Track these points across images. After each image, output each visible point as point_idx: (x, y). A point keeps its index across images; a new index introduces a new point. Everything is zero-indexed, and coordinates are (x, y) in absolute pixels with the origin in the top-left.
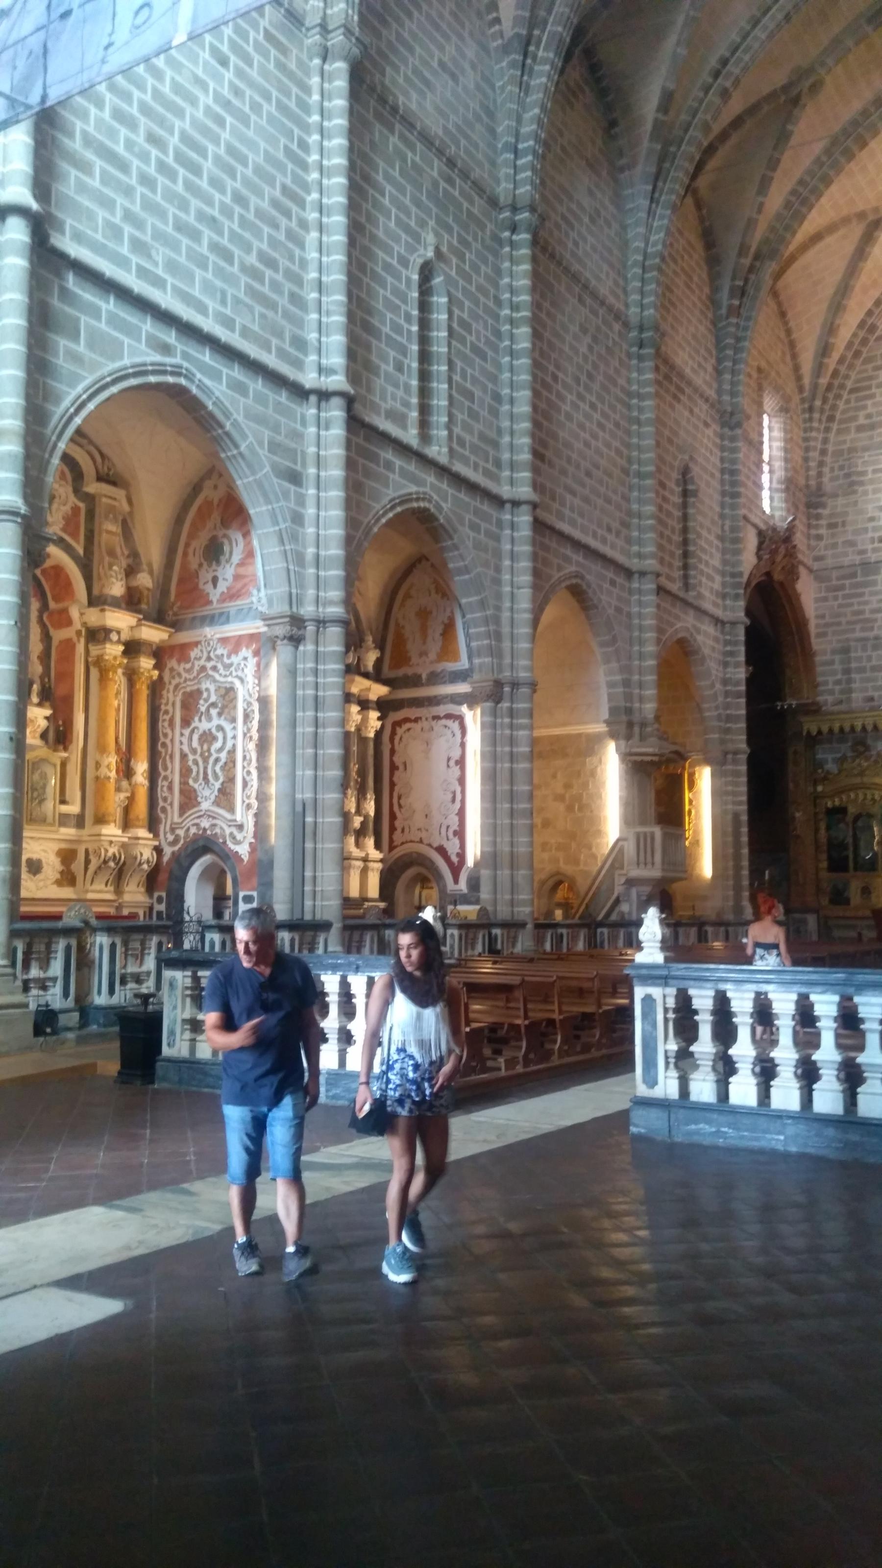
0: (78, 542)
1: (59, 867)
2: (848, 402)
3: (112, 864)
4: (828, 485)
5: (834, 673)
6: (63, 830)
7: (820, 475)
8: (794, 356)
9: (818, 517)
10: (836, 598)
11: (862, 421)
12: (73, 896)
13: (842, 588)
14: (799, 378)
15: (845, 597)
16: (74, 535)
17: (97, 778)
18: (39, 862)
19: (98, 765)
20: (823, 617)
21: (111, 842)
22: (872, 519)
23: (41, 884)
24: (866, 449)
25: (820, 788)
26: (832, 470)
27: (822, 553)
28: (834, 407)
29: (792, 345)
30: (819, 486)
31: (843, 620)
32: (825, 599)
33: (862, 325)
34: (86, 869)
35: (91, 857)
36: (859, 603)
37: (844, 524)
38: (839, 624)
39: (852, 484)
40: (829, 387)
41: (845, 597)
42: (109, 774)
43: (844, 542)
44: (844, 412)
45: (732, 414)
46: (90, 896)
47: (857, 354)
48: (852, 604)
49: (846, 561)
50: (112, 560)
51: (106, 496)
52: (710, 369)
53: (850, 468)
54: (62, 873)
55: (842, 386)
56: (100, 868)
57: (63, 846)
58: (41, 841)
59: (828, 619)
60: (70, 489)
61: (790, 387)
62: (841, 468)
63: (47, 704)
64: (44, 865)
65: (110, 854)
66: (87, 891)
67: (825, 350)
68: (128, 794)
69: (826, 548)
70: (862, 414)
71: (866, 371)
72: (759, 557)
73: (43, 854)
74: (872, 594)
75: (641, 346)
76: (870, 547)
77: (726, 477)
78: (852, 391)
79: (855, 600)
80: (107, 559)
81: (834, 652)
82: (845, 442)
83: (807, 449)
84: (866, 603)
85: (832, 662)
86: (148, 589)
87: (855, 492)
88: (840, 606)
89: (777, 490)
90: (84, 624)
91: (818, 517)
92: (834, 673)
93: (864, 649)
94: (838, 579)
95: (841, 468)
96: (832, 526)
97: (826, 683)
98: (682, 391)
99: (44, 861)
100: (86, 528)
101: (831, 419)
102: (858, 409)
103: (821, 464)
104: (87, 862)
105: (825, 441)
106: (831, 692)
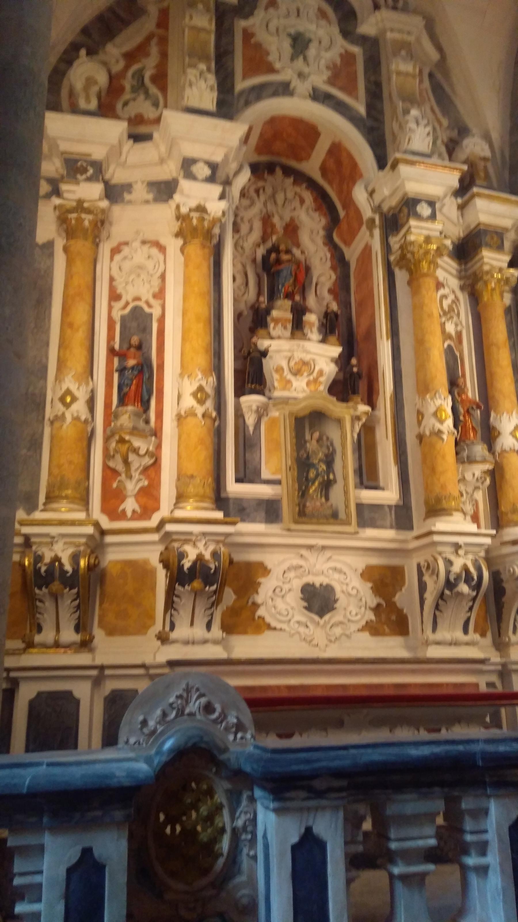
0: (357, 98)
1: (373, 601)
3: (464, 588)
6: (370, 532)
12: (404, 654)
16: (351, 90)
17: (420, 438)
18: (329, 589)
19: (420, 415)
21: (457, 547)
23: (338, 631)
34: (422, 601)
35: (426, 578)
42: (438, 426)
46: (434, 652)
50: (408, 105)
51: (392, 30)
54: (377, 609)
56: (442, 596)
57: (375, 561)
58: (328, 553)
60: (335, 30)
63: (333, 339)
64: (339, 594)
65: (457, 568)
66: (427, 643)
68: (488, 467)
73: (336, 576)
80: (400, 105)
86: (485, 159)
90: (377, 209)
99: (338, 588)
100: (367, 80)
104: (422, 587)
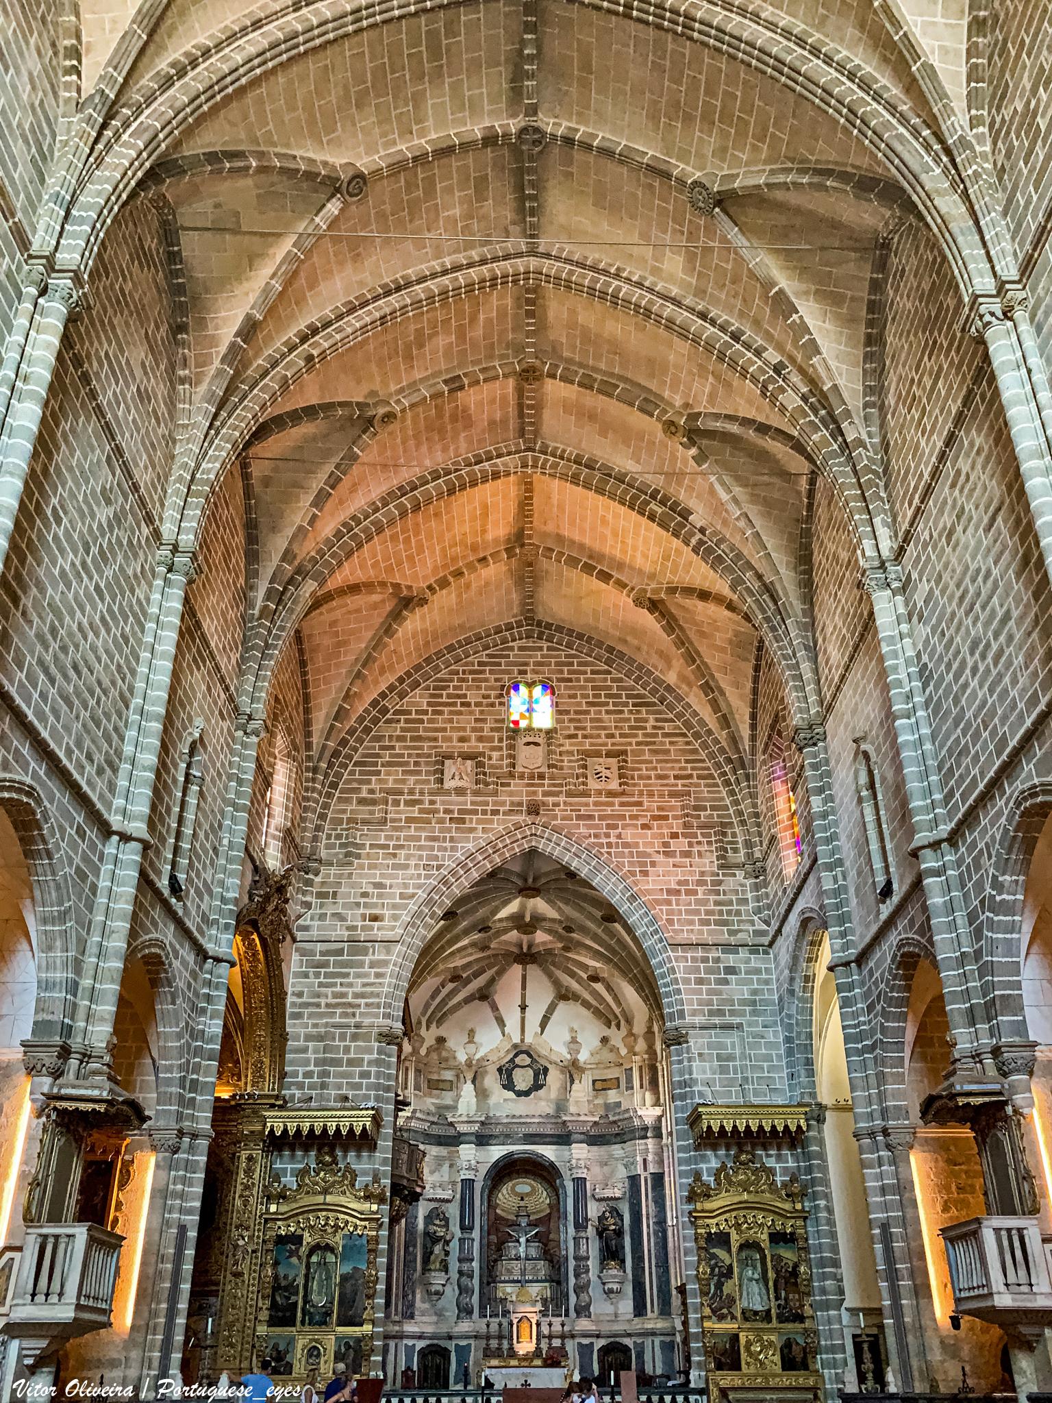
2: (352, 773)
4: (323, 854)
5: (307, 1062)
7: (315, 839)
8: (307, 711)
9: (309, 883)
10: (317, 975)
11: (364, 794)
13: (325, 965)
14: (308, 734)
15: (326, 975)
20: (300, 995)
22: (365, 895)
24: (364, 822)
25: (273, 1208)
26: (329, 837)
27: (308, 923)
28: (339, 775)
29: (306, 698)
30: (314, 850)
31: (323, 1001)
32: (306, 976)
33: (374, 703)
36: (341, 984)
37: (335, 894)
38: (318, 1005)
39: (348, 855)
40: (336, 754)
41: (326, 975)
43: (333, 915)
44: (348, 782)
45: (250, 718)
47: (367, 730)
48: (334, 985)
49: (333, 935)
52: (233, 661)
53: (347, 838)
55: (350, 757)
59: (304, 1000)
61: (299, 739)
62: (338, 837)
67: (340, 715)
69: (312, 919)
70: (364, 787)
71: (374, 748)
72: (251, 899)
74: (358, 976)
75: (170, 570)
76: (360, 924)
77: (233, 784)
78: (356, 764)
79: (339, 981)
81: (309, 1038)
82: (344, 811)
83: (306, 809)
84: (350, 985)
85: (305, 1050)
87: (351, 864)
88: (321, 985)
89: (274, 837)
91: (309, 883)
92: (307, 1062)
93: (343, 1037)
94: (322, 954)
95: (338, 837)
96: (320, 895)
97: (295, 1074)
98: (204, 662)
101: (334, 785)
102: (360, 782)
103: (318, 828)
105: (326, 806)
106: (300, 1086)
